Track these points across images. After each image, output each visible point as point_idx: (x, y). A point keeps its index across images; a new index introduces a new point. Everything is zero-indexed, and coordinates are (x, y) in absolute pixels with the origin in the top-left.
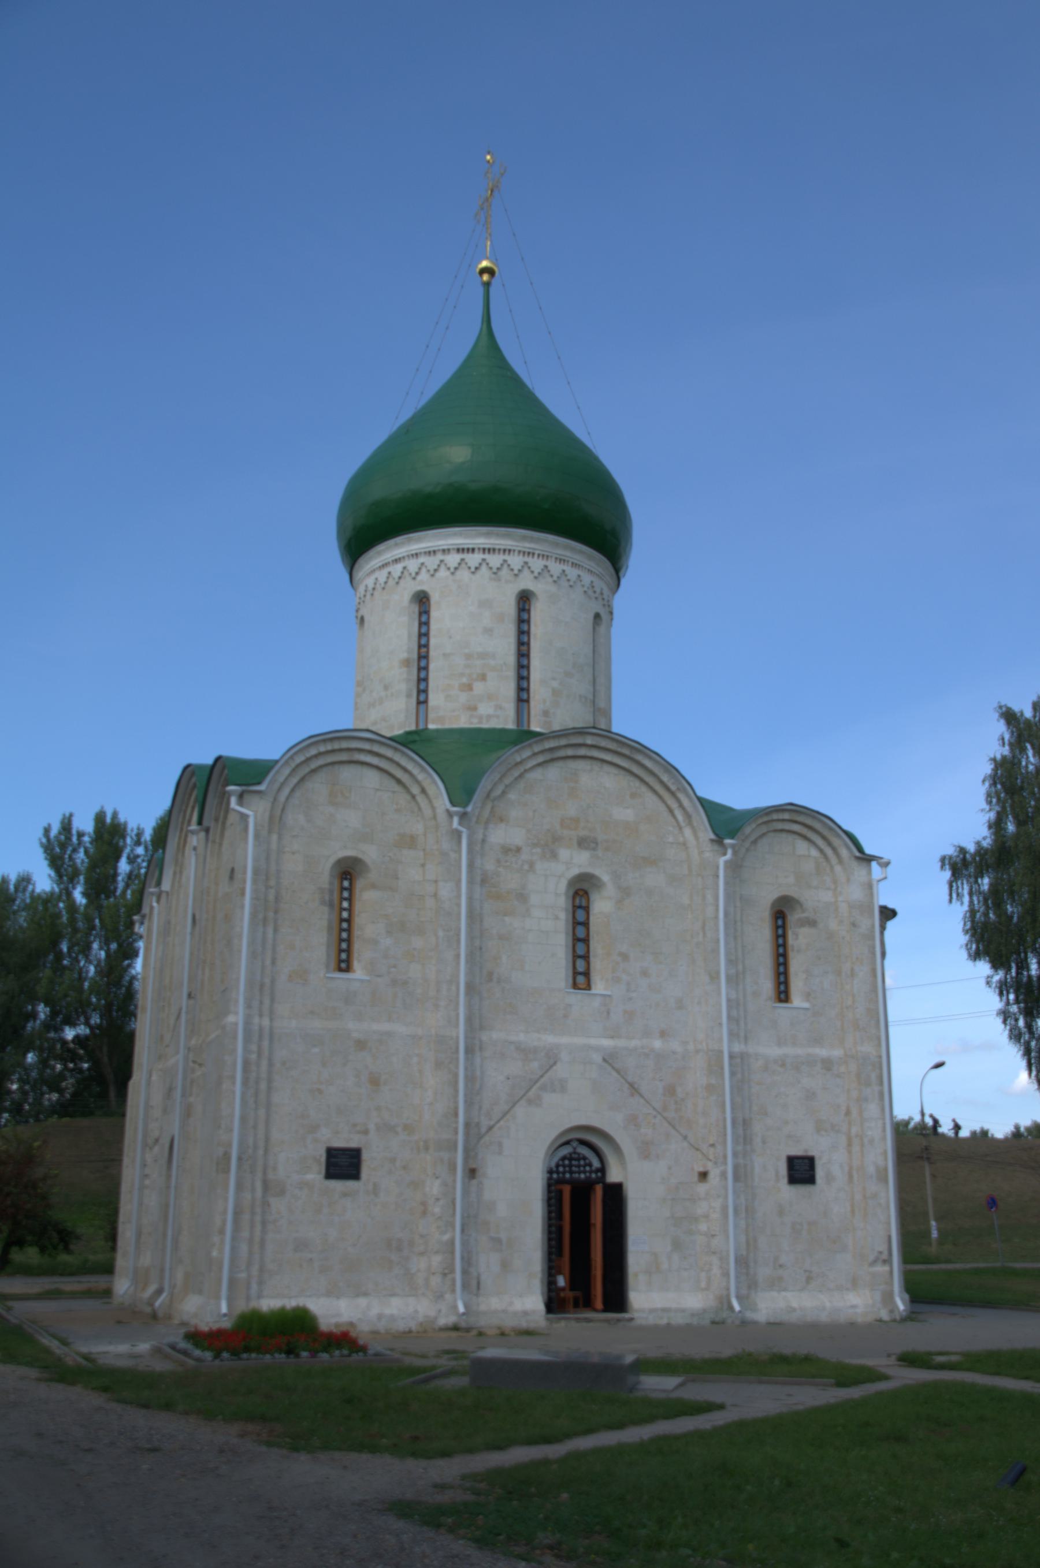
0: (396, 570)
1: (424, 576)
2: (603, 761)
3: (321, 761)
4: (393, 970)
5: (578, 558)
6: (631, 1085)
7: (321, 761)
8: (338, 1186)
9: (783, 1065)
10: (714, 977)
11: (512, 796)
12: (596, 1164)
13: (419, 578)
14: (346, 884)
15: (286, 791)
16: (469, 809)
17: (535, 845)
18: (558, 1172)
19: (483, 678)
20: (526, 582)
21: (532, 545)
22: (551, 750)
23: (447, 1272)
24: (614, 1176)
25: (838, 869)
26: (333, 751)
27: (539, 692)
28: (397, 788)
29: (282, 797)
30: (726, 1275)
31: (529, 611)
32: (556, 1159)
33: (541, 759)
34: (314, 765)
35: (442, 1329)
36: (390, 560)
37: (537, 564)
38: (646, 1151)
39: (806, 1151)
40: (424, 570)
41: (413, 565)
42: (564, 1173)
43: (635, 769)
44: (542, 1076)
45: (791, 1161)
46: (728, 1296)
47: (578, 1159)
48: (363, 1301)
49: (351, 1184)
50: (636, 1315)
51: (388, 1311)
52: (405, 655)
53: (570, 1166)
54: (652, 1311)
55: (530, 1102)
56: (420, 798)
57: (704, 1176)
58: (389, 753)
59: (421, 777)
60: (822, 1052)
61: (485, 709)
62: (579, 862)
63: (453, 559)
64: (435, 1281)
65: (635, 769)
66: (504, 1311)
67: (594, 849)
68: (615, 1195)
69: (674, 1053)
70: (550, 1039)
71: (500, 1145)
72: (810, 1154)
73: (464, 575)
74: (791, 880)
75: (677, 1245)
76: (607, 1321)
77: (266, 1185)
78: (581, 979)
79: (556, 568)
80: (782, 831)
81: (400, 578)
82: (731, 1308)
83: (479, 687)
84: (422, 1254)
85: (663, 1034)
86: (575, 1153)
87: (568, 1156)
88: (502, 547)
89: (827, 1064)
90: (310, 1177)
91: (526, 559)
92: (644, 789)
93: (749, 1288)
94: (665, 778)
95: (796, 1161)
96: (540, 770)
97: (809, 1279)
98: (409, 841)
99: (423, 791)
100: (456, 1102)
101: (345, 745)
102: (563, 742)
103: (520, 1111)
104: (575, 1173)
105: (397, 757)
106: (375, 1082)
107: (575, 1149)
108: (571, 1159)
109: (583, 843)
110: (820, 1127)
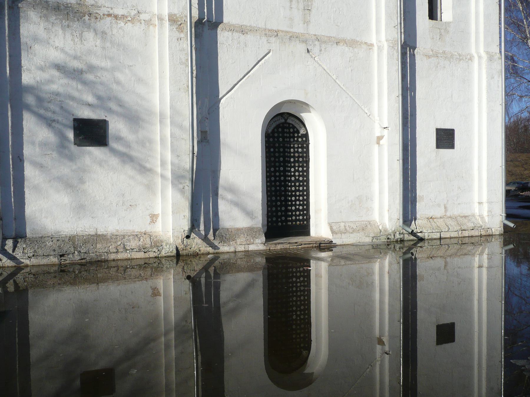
18: (274, 137)
32: (272, 128)
42: (278, 137)
53: (283, 132)
86: (286, 122)
87: (281, 125)
104: (287, 137)
107: (286, 120)
108: (283, 128)
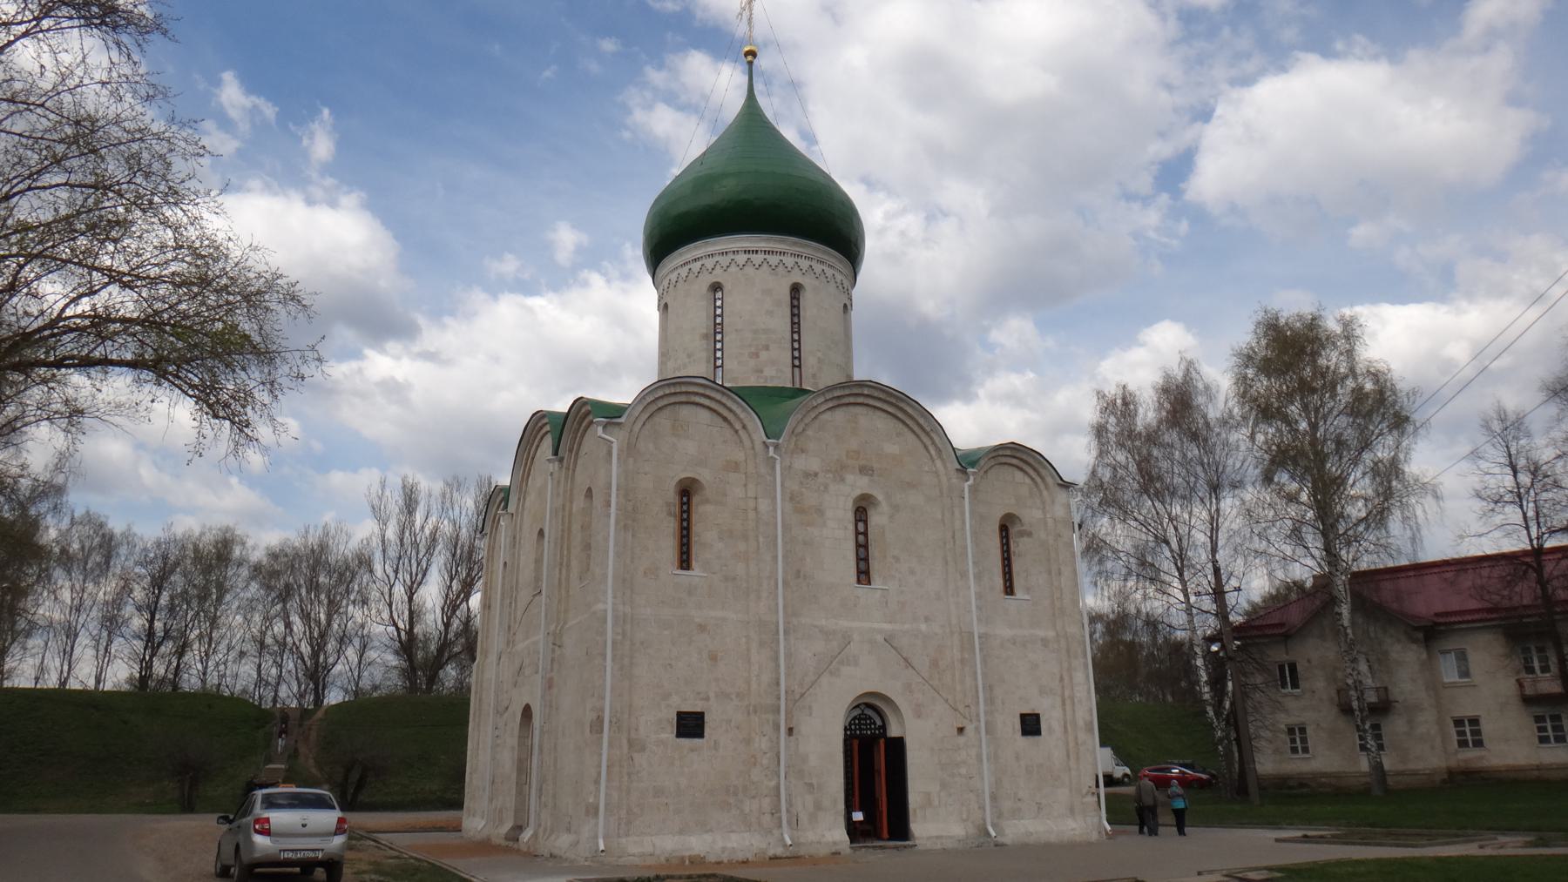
0: (697, 266)
1: (718, 270)
2: (875, 407)
3: (665, 402)
4: (725, 568)
5: (832, 261)
6: (906, 660)
7: (665, 402)
8: (686, 742)
9: (1014, 644)
10: (964, 575)
11: (810, 432)
12: (879, 723)
13: (714, 272)
14: (685, 499)
15: (639, 424)
16: (781, 441)
17: (828, 471)
18: (851, 729)
20: (797, 277)
21: (801, 250)
22: (839, 397)
23: (775, 811)
24: (894, 731)
25: (1045, 493)
26: (675, 394)
27: (809, 361)
28: (725, 425)
29: (636, 429)
30: (982, 808)
31: (798, 299)
32: (849, 719)
33: (830, 404)
34: (661, 403)
35: (771, 858)
36: (690, 260)
37: (804, 264)
38: (918, 715)
39: (1034, 710)
40: (718, 267)
41: (709, 263)
43: (900, 415)
44: (840, 653)
45: (1023, 717)
46: (985, 824)
47: (865, 719)
48: (708, 837)
49: (696, 741)
50: (917, 842)
51: (729, 845)
52: (705, 331)
54: (929, 838)
55: (831, 673)
56: (741, 432)
57: (961, 730)
58: (718, 396)
59: (742, 416)
60: (1041, 633)
61: (769, 372)
62: (858, 485)
63: (741, 258)
64: (767, 819)
65: (900, 415)
66: (819, 843)
67: (872, 475)
68: (897, 747)
69: (936, 634)
70: (844, 623)
71: (810, 707)
72: (1036, 712)
73: (749, 270)
75: (944, 785)
76: (897, 848)
77: (631, 743)
78: (863, 577)
79: (818, 268)
80: (1005, 464)
81: (699, 273)
82: (988, 834)
83: (764, 355)
84: (754, 797)
85: (927, 619)
88: (779, 250)
90: (664, 736)
91: (796, 260)
92: (906, 430)
93: (999, 817)
94: (922, 421)
95: (1028, 718)
96: (829, 413)
98: (734, 467)
99: (744, 427)
100: (778, 673)
101: (684, 389)
102: (847, 392)
103: (825, 680)
104: (864, 730)
105: (724, 400)
106: (714, 658)
107: (863, 711)
108: (860, 719)
109: (864, 470)
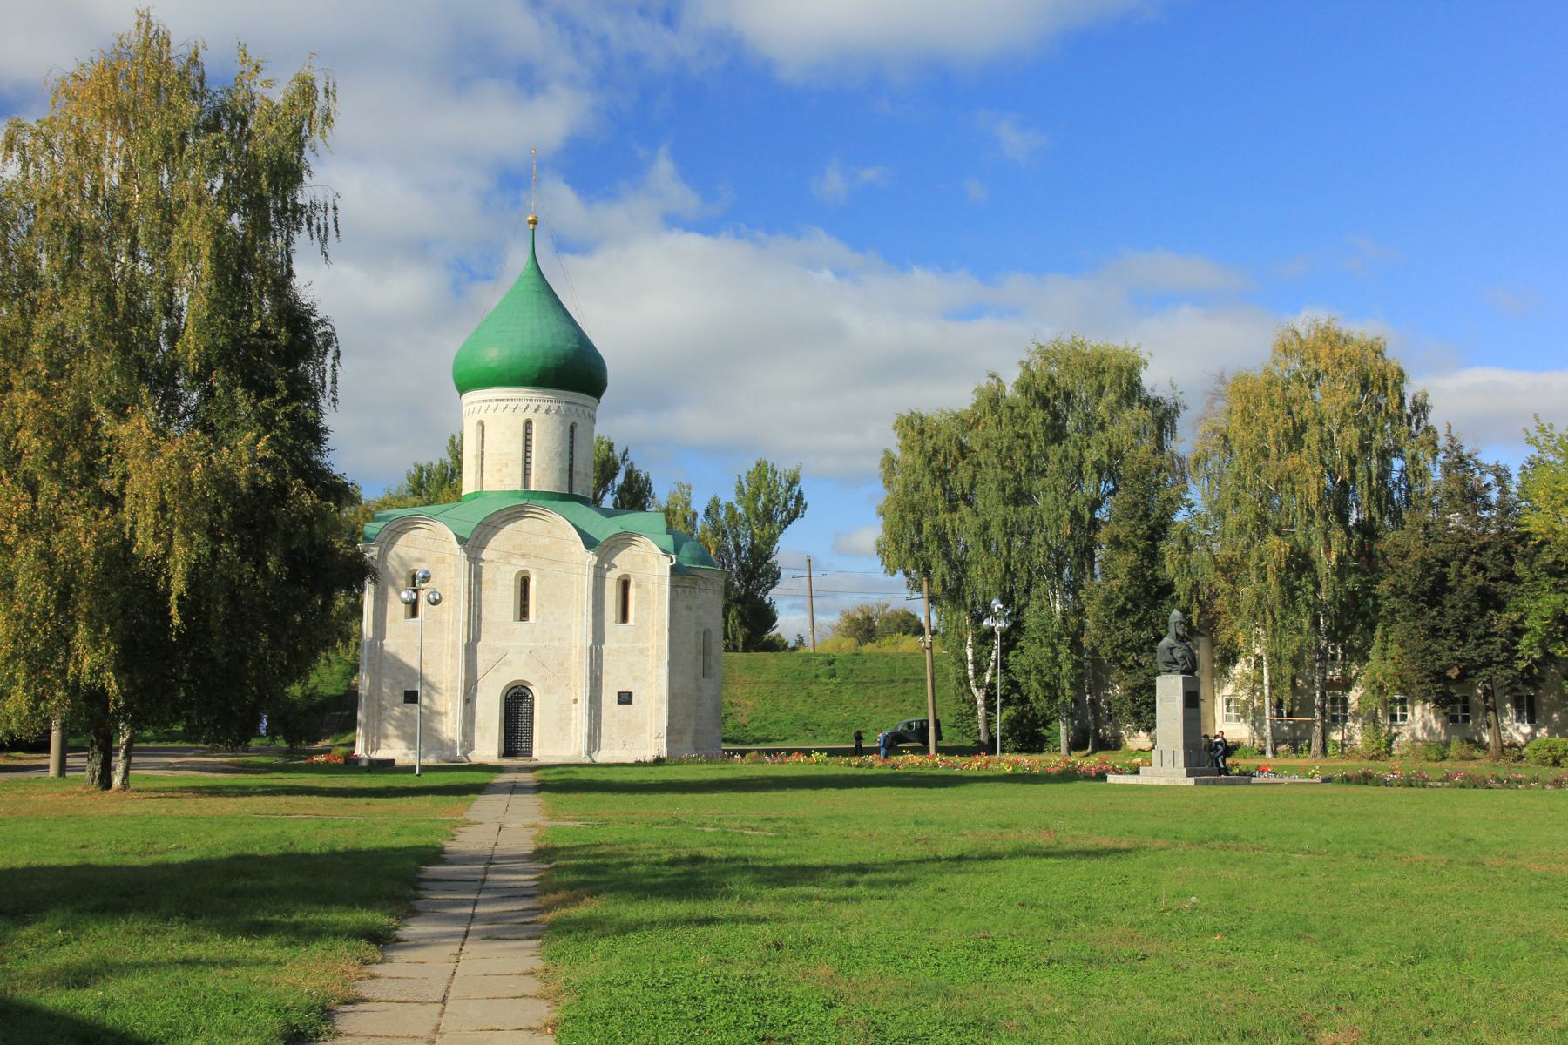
19: (507, 465)
20: (529, 415)
22: (508, 515)
45: (619, 694)
61: (508, 481)
62: (520, 565)
63: (494, 405)
74: (629, 566)
75: (561, 730)
83: (505, 470)
89: (642, 651)
97: (625, 745)
109: (523, 555)
110: (635, 679)
